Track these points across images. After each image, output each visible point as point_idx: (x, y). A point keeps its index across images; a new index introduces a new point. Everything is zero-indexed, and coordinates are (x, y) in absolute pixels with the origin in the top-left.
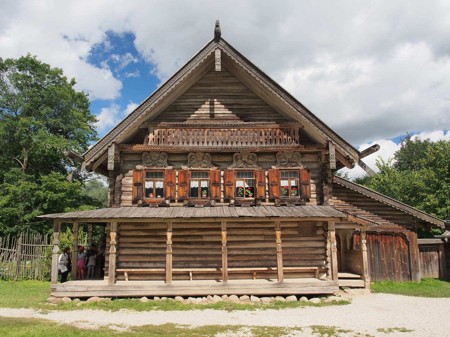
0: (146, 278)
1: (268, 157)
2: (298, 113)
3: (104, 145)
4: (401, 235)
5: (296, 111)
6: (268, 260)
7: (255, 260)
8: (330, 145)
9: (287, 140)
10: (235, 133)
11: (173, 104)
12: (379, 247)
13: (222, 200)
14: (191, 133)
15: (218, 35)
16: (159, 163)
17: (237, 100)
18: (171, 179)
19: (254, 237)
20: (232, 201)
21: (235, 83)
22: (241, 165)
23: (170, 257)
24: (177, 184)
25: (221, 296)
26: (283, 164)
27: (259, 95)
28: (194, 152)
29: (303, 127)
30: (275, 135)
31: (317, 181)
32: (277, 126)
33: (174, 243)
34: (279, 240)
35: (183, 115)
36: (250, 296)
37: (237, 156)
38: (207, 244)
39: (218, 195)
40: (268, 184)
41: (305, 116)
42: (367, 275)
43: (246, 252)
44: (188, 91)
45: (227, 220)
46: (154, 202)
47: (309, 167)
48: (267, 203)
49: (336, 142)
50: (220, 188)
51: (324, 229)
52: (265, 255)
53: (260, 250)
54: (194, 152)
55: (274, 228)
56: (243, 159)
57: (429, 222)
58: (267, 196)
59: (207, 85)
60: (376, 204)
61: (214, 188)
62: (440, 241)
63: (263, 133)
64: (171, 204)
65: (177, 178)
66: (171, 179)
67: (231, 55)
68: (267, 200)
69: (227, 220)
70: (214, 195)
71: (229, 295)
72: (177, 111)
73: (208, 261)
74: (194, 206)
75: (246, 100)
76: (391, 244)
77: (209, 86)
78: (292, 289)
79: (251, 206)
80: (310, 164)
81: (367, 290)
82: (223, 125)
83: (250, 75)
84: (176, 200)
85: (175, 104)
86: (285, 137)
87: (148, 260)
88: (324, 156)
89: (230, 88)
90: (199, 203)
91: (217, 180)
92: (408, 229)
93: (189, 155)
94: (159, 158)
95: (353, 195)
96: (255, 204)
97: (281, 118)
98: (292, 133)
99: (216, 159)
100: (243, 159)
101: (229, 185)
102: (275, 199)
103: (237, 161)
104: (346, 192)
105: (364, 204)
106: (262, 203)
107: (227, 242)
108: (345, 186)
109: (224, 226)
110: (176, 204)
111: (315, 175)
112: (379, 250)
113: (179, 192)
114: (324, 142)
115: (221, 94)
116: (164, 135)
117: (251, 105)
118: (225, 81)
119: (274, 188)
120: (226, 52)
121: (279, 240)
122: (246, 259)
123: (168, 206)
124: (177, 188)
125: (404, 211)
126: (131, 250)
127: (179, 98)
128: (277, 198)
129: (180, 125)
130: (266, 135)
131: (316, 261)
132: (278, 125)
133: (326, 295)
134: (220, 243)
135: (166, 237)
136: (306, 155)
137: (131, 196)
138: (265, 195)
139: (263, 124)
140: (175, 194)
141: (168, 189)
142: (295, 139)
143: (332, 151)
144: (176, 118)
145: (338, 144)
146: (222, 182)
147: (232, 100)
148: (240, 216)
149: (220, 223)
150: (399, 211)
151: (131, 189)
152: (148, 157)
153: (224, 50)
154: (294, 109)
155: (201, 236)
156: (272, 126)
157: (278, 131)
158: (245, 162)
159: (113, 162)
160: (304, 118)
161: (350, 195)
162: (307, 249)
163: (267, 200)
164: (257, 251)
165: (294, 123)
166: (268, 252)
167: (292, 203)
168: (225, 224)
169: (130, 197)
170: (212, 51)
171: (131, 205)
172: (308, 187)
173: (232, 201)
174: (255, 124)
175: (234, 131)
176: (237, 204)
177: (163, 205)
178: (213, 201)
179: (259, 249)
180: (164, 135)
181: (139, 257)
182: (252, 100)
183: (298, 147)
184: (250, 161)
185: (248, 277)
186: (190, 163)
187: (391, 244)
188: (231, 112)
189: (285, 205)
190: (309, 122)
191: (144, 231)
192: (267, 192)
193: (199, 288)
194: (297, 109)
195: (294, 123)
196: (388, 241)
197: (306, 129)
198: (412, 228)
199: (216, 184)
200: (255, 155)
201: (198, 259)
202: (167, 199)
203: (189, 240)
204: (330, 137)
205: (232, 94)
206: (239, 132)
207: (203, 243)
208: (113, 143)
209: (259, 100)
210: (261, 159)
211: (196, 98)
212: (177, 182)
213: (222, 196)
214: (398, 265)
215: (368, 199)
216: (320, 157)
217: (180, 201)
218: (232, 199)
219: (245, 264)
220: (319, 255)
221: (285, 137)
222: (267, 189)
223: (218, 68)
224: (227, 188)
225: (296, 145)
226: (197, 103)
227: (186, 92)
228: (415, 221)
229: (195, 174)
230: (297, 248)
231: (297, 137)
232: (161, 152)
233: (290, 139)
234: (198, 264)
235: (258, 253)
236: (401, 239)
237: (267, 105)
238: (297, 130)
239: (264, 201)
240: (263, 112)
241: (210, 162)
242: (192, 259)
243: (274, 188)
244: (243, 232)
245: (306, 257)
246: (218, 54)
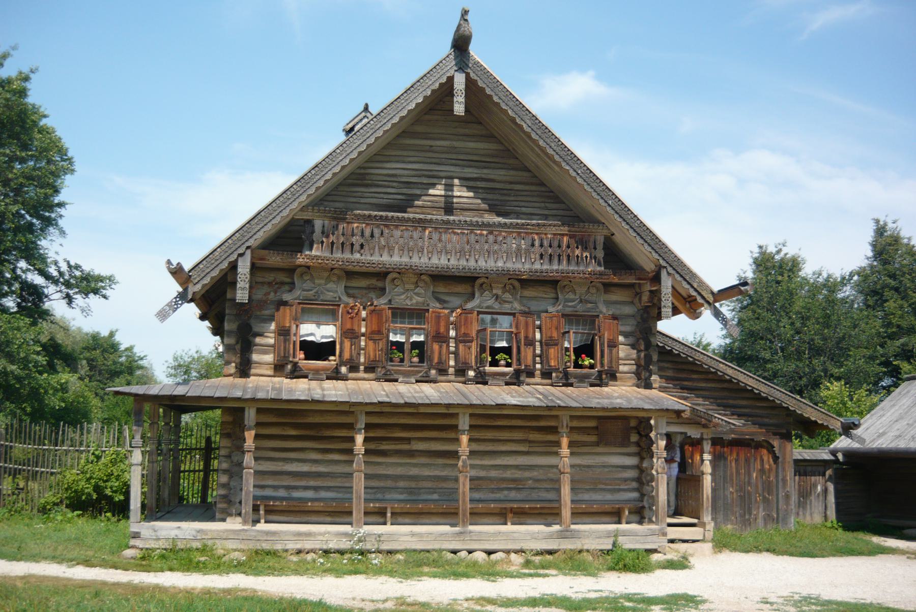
0: (298, 519)
1: (541, 289)
2: (609, 209)
3: (230, 252)
4: (765, 444)
5: (604, 204)
6: (534, 488)
7: (509, 489)
8: (664, 274)
9: (582, 258)
10: (483, 239)
11: (358, 171)
13: (451, 370)
14: (397, 233)
15: (461, 44)
16: (328, 291)
17: (485, 171)
18: (352, 324)
19: (509, 444)
20: (471, 373)
21: (482, 136)
22: (490, 302)
23: (360, 479)
24: (363, 335)
26: (570, 304)
27: (527, 165)
28: (399, 273)
29: (613, 234)
30: (559, 246)
31: (631, 340)
32: (565, 230)
33: (368, 452)
34: (565, 451)
35: (376, 195)
36: (508, 552)
37: (482, 285)
38: (420, 456)
39: (444, 358)
40: (541, 342)
41: (620, 216)
42: (707, 518)
43: (493, 474)
44: (389, 145)
45: (471, 411)
46: (317, 371)
47: (617, 312)
48: (537, 379)
49: (674, 269)
50: (448, 346)
51: (639, 433)
52: (530, 479)
53: (521, 469)
54: (399, 273)
55: (556, 428)
56: (495, 291)
57: (816, 422)
58: (538, 366)
59: (425, 136)
60: (725, 385)
61: (436, 347)
62: (827, 456)
63: (537, 243)
64: (351, 375)
65: (363, 323)
66: (352, 324)
67: (484, 86)
68: (538, 373)
69: (471, 411)
70: (436, 360)
71: (470, 552)
72: (367, 186)
73: (420, 489)
74: (396, 381)
75: (503, 172)
76: (747, 461)
77: (430, 139)
79: (507, 384)
80: (618, 306)
81: (709, 545)
82: (460, 221)
83: (520, 127)
84: (362, 368)
85: (362, 171)
86: (577, 252)
87: (303, 483)
88: (648, 293)
89: (472, 145)
90: (407, 374)
91: (442, 330)
92: (775, 434)
93: (390, 276)
94: (328, 280)
95: (685, 367)
96: (515, 380)
97: (568, 213)
98: (591, 245)
100: (495, 291)
101: (465, 342)
102: (551, 374)
103: (481, 294)
104: (672, 362)
105: (704, 385)
106: (529, 380)
107: (470, 452)
108: (671, 351)
109: (464, 422)
110: (361, 374)
111: (628, 329)
112: (725, 472)
113: (367, 349)
114: (649, 267)
115: (454, 156)
116: (343, 235)
117: (511, 183)
118: (462, 131)
119: (552, 351)
120: (475, 78)
121: (565, 451)
122: (493, 486)
123: (345, 378)
124: (363, 343)
125: (773, 401)
126: (269, 463)
127: (369, 161)
128: (557, 370)
129: (376, 216)
130: (541, 246)
131: (622, 493)
132: (566, 228)
134: (455, 455)
135: (352, 440)
136: (613, 289)
137: (272, 355)
138: (535, 363)
139: (538, 225)
140: (359, 354)
141: (347, 344)
142: (595, 258)
143: (667, 284)
144: (363, 200)
145: (678, 272)
146: (452, 333)
147: (476, 171)
149: (455, 415)
150: (766, 399)
151: (272, 341)
152: (305, 278)
153: (472, 75)
154: (601, 201)
156: (554, 229)
157: (565, 239)
158: (497, 297)
159: (247, 286)
160: (619, 220)
161: (680, 367)
162: (606, 470)
163: (538, 373)
164: (513, 471)
165: (596, 227)
166: (534, 474)
168: (467, 419)
169: (269, 358)
170: (449, 75)
171: (271, 372)
172: (615, 350)
173: (471, 373)
174: (523, 225)
175: (481, 235)
176: (481, 379)
177: (335, 375)
178: (433, 372)
179: (517, 467)
180: (343, 235)
181: (287, 477)
182: (512, 173)
183: (601, 274)
184: (507, 296)
185: (496, 519)
186: (390, 293)
187: (747, 461)
188: (471, 194)
189: (571, 385)
190: (627, 227)
191: (296, 426)
192: (538, 359)
193: (414, 539)
194: (606, 202)
195: (596, 227)
196: (742, 456)
197: (618, 238)
198: (784, 431)
199: (441, 338)
200: (517, 284)
201: (401, 484)
202: (342, 363)
203: (384, 447)
204: (663, 259)
205: (475, 158)
206: (491, 238)
207: (411, 454)
208: (248, 248)
209: (526, 174)
210: (528, 293)
211: (404, 162)
212: (363, 330)
213: (452, 363)
215: (710, 376)
216: (638, 294)
217: (370, 369)
218: (471, 368)
219: (492, 496)
220: (628, 482)
221: (577, 252)
222: (538, 351)
223: (459, 108)
224: (461, 346)
225: (598, 269)
226: (406, 172)
227: (384, 148)
228: (791, 420)
229: (400, 313)
230: (589, 466)
231: (600, 254)
232: (332, 269)
233: (586, 257)
234: (401, 493)
235: (516, 476)
236: (765, 451)
237: (542, 184)
238: (600, 240)
239: (531, 374)
240: (535, 199)
241: (430, 294)
242: (389, 483)
243: (552, 351)
244: (490, 435)
245: (606, 484)
246: (460, 81)
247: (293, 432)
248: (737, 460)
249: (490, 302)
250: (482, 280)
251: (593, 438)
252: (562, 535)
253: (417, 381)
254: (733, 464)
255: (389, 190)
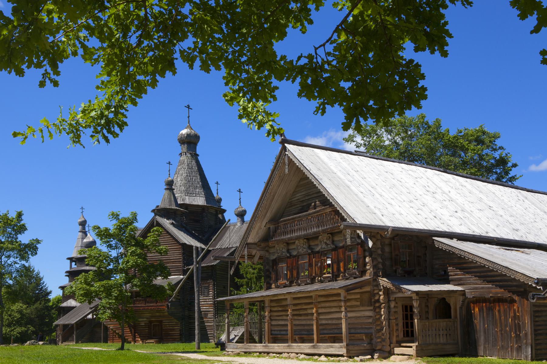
12: (493, 315)
25: (288, 353)
43: (330, 322)
78: (322, 350)
99: (312, 243)
133: (338, 356)
148: (287, 293)
155: (306, 309)
158: (326, 243)
167: (351, 277)
191: (280, 306)
203: (301, 313)
214: (511, 336)
244: (327, 304)
247: (280, 309)
248: (499, 311)
249: (324, 246)
250: (320, 237)
251: (358, 303)
252: (314, 347)
253: (305, 284)
254: (497, 313)
255: (298, 206)
